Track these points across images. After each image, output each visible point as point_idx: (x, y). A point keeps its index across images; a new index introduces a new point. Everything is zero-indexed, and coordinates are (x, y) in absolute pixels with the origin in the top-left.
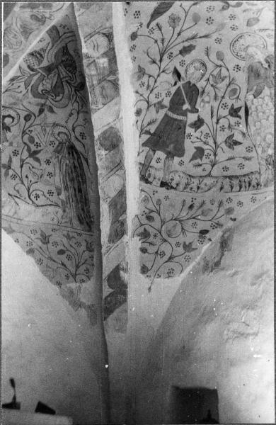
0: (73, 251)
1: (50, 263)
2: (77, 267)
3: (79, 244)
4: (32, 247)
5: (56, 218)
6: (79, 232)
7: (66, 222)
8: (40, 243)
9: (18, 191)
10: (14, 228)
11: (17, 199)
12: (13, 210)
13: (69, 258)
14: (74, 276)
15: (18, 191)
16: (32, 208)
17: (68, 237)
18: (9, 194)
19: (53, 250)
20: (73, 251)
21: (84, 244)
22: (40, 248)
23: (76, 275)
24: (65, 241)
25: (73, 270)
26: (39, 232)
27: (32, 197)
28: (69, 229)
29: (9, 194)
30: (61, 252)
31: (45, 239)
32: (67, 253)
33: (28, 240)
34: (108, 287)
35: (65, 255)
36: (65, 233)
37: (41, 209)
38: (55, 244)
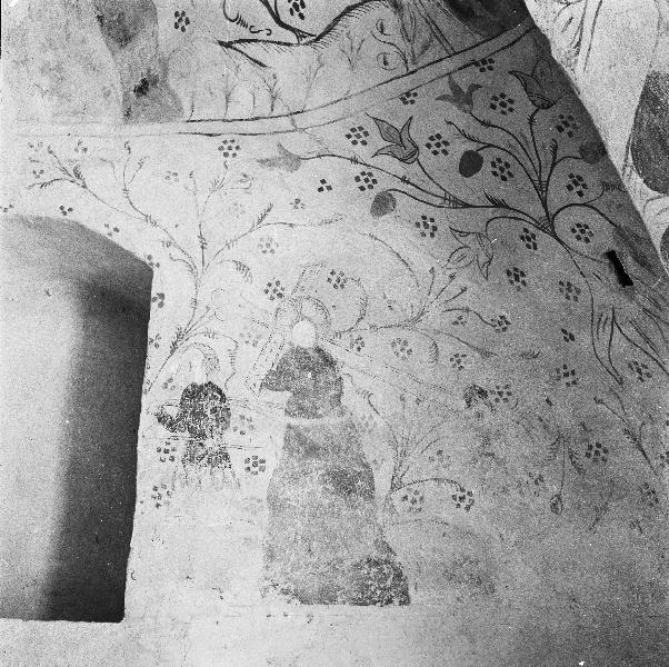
0: (496, 137)
1: (461, 218)
2: (542, 188)
3: (502, 102)
4: (378, 189)
5: (387, 48)
6: (479, 54)
7: (425, 47)
8: (397, 167)
9: (239, 20)
10: (296, 150)
11: (251, 49)
12: (264, 96)
13: (503, 172)
14: (548, 224)
15: (239, 20)
16: (304, 53)
17: (461, 97)
18: (221, 43)
19: (442, 167)
20: (496, 137)
21: (515, 89)
22: (403, 180)
23: (551, 219)
24: (454, 112)
25: (536, 210)
26: (371, 127)
27: (285, 17)
28: (447, 65)
29: (221, 43)
30: (470, 164)
31: (401, 145)
32: (488, 156)
33: (357, 170)
34: (653, 194)
35: (487, 168)
36: (443, 87)
37: (331, 48)
38: (438, 143)
